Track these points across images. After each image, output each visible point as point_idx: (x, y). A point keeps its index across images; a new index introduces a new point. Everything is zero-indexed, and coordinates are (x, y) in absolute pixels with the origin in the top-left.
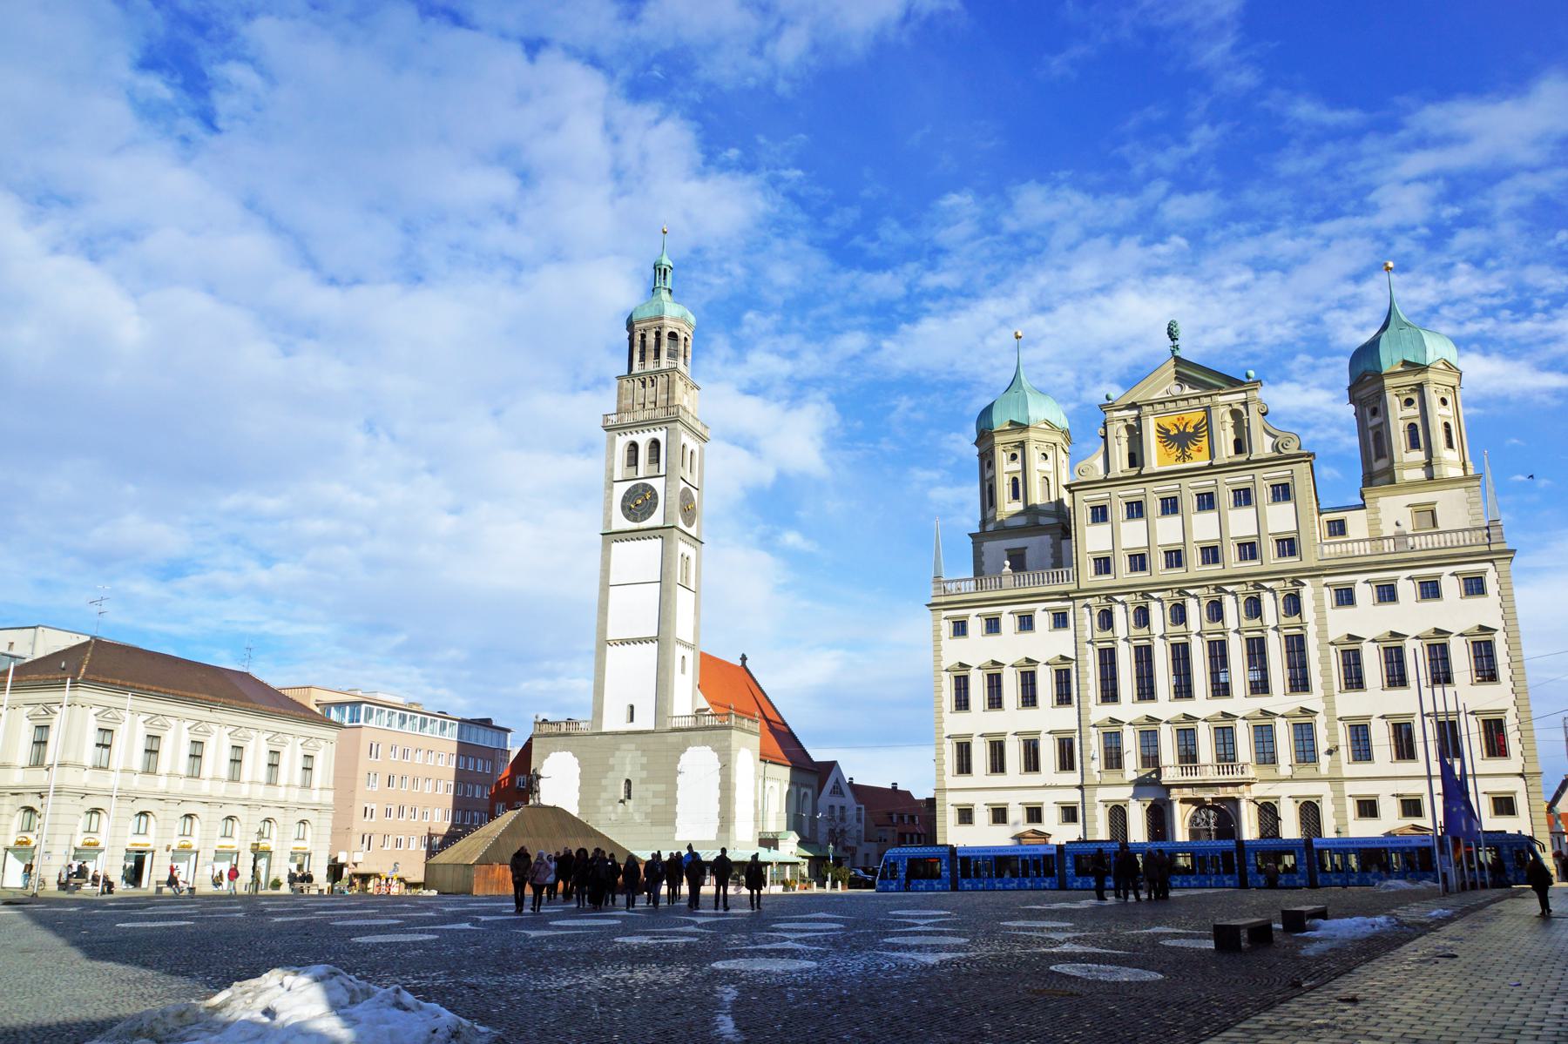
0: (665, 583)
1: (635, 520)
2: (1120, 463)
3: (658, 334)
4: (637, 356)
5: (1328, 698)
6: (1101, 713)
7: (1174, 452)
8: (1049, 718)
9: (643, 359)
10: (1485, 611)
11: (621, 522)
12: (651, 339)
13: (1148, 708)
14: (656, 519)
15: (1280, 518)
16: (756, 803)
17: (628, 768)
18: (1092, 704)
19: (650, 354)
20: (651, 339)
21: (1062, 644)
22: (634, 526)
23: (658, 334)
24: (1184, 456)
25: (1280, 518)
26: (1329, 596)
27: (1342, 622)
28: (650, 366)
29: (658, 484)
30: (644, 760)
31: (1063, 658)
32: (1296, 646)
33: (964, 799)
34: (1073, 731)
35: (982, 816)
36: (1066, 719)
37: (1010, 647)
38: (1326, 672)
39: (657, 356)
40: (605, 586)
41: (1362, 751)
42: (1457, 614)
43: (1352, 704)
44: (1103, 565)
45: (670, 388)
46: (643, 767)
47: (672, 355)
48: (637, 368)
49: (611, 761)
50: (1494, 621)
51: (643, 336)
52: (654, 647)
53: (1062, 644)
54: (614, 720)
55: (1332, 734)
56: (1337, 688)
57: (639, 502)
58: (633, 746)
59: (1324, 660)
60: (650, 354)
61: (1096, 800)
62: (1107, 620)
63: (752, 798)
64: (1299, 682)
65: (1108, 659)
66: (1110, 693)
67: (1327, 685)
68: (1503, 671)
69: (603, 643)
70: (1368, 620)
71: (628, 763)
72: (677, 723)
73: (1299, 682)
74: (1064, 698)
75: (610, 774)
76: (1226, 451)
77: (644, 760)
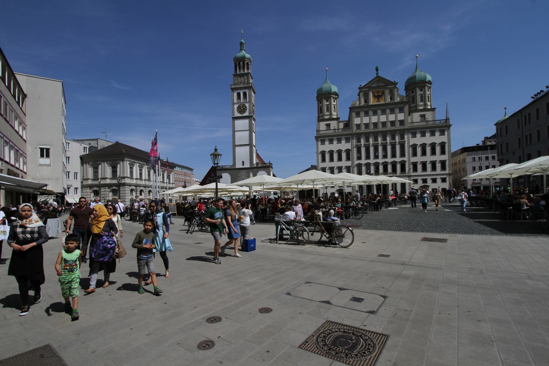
0: (251, 130)
2: (363, 103)
3: (244, 63)
4: (238, 69)
6: (357, 162)
7: (376, 100)
9: (240, 69)
10: (444, 139)
11: (237, 114)
12: (241, 63)
14: (247, 114)
18: (355, 160)
19: (242, 68)
20: (241, 63)
21: (348, 146)
22: (241, 115)
23: (244, 63)
24: (379, 101)
25: (401, 116)
26: (410, 136)
27: (413, 141)
28: (242, 72)
29: (247, 105)
37: (335, 146)
38: (409, 152)
39: (244, 69)
40: (234, 131)
41: (415, 169)
42: (438, 139)
43: (413, 160)
44: (358, 126)
45: (248, 78)
47: (248, 69)
48: (238, 72)
50: (446, 141)
51: (239, 64)
52: (248, 147)
53: (348, 146)
54: (239, 165)
55: (409, 167)
57: (242, 109)
59: (408, 150)
60: (242, 68)
62: (359, 141)
64: (403, 155)
66: (359, 158)
68: (447, 152)
69: (235, 146)
70: (419, 140)
73: (403, 155)
74: (348, 159)
76: (388, 100)
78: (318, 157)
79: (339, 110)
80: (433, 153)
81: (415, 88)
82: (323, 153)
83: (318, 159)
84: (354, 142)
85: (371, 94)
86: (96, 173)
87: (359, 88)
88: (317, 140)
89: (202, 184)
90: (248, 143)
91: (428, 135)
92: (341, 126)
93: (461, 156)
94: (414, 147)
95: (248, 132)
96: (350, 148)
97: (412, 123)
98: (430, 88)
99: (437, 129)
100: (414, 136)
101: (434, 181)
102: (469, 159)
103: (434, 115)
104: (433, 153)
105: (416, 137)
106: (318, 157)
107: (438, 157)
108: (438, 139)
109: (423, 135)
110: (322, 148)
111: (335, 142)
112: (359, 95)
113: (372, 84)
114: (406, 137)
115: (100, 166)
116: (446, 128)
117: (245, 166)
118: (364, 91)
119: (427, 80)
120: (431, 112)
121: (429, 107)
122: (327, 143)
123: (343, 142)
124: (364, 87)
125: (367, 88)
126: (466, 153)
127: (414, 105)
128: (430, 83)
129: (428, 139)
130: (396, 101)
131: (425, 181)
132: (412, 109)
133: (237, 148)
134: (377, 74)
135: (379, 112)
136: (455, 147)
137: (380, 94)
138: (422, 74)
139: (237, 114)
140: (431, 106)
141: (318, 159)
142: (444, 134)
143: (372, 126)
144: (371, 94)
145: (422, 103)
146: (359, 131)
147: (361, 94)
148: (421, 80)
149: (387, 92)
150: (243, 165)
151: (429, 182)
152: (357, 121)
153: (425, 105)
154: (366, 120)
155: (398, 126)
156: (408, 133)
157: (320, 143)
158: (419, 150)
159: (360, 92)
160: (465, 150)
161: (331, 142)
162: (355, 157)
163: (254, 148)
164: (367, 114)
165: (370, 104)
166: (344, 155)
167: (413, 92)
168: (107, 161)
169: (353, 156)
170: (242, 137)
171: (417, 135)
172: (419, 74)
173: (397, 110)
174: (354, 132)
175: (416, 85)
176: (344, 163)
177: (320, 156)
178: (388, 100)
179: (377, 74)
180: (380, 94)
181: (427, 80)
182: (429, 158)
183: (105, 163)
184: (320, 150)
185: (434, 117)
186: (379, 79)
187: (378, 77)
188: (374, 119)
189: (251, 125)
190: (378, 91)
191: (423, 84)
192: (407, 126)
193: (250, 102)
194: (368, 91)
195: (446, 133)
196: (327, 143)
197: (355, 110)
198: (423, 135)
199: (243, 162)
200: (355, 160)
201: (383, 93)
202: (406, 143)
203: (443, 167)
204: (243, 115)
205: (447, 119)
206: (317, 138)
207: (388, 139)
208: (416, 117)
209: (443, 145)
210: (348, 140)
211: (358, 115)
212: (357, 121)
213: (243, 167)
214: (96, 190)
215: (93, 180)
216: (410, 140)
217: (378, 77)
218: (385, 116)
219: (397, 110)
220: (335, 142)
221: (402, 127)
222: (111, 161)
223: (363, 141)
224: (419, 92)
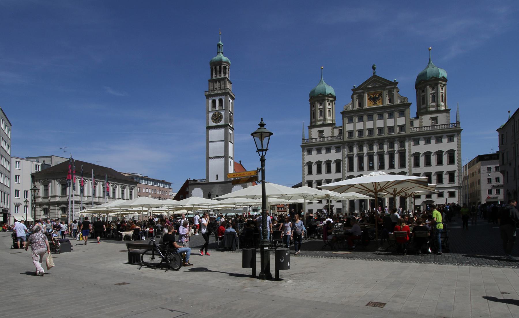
0: (226, 141)
1: (216, 123)
2: (356, 106)
7: (372, 103)
10: (453, 146)
14: (222, 123)
15: (401, 121)
18: (346, 172)
22: (216, 124)
25: (401, 121)
26: (412, 143)
27: (415, 149)
38: (410, 163)
40: (208, 142)
52: (223, 159)
54: (212, 179)
59: (410, 159)
62: (351, 150)
67: (410, 166)
69: (208, 158)
70: (422, 148)
76: (387, 102)
78: (303, 169)
79: (332, 113)
80: (440, 162)
81: (425, 87)
82: (310, 165)
83: (303, 172)
84: (346, 151)
85: (366, 96)
86: (46, 190)
87: (352, 90)
88: (303, 150)
89: (178, 198)
91: (445, 140)
92: (337, 132)
93: (477, 166)
94: (416, 156)
95: (223, 143)
96: (341, 159)
97: (421, 127)
98: (444, 85)
99: (445, 135)
100: (417, 143)
102: (484, 169)
103: (448, 117)
104: (440, 162)
105: (418, 144)
106: (303, 169)
107: (445, 168)
108: (445, 146)
109: (428, 142)
110: (308, 158)
111: (323, 152)
112: (352, 97)
113: (368, 85)
114: (407, 144)
115: (50, 184)
116: (456, 134)
118: (358, 93)
119: (440, 76)
120: (444, 114)
121: (443, 108)
122: (314, 153)
123: (333, 151)
124: (358, 88)
125: (362, 89)
126: (480, 162)
127: (424, 106)
128: (444, 79)
129: (433, 147)
130: (395, 103)
132: (422, 111)
133: (210, 160)
134: (374, 73)
135: (376, 116)
136: (467, 155)
137: (377, 96)
138: (435, 69)
139: (211, 123)
140: (446, 107)
141: (303, 172)
142: (453, 141)
143: (366, 133)
144: (366, 96)
145: (434, 104)
146: (351, 139)
147: (355, 96)
148: (433, 77)
149: (385, 93)
150: (217, 178)
152: (349, 127)
153: (438, 105)
154: (360, 126)
155: (397, 132)
156: (410, 140)
157: (306, 153)
158: (422, 160)
159: (353, 94)
160: (481, 158)
161: (319, 151)
163: (230, 160)
164: (361, 119)
165: (364, 107)
166: (333, 167)
167: (423, 91)
168: (57, 179)
170: (217, 148)
171: (420, 142)
172: (431, 70)
173: (397, 114)
174: (345, 140)
175: (426, 83)
176: (334, 175)
177: (306, 168)
178: (387, 102)
179: (374, 73)
180: (377, 96)
181: (440, 76)
182: (434, 169)
183: (55, 181)
184: (306, 161)
185: (448, 120)
186: (375, 79)
187: (374, 76)
188: (370, 125)
189: (226, 133)
190: (375, 93)
191: (435, 81)
192: (409, 131)
193: (226, 110)
194: (363, 93)
195: (456, 139)
196: (314, 153)
197: (348, 115)
198: (428, 142)
199: (217, 176)
200: (346, 172)
201: (381, 94)
202: (407, 151)
203: (452, 179)
204: (219, 124)
205: (458, 123)
206: (303, 147)
207: (386, 147)
208: (426, 120)
209: (451, 153)
210: (338, 150)
211: (350, 120)
212: (349, 127)
214: (64, 207)
215: (43, 198)
216: (410, 148)
217: (374, 76)
218: (383, 121)
219: (397, 114)
220: (323, 152)
221: (402, 134)
222: (61, 178)
223: (355, 150)
224: (430, 91)
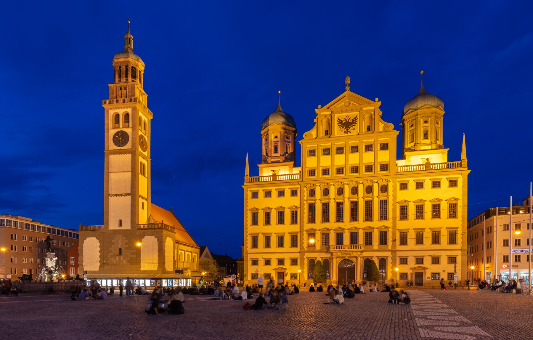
5: (394, 223)
8: (288, 228)
13: (326, 225)
16: (174, 257)
17: (120, 244)
21: (295, 201)
30: (127, 241)
31: (295, 206)
32: (384, 204)
33: (254, 256)
34: (298, 233)
35: (261, 262)
36: (295, 228)
46: (126, 244)
49: (113, 241)
52: (129, 198)
53: (295, 201)
56: (398, 219)
58: (121, 236)
59: (394, 209)
61: (305, 257)
63: (172, 255)
65: (312, 208)
66: (312, 220)
67: (394, 218)
71: (120, 242)
72: (142, 227)
75: (113, 246)
77: (127, 241)
90: (129, 192)
101: (436, 260)
117: (124, 227)
131: (419, 260)
150: (120, 225)
151: (427, 262)
162: (306, 219)
169: (302, 217)
213: (120, 228)
